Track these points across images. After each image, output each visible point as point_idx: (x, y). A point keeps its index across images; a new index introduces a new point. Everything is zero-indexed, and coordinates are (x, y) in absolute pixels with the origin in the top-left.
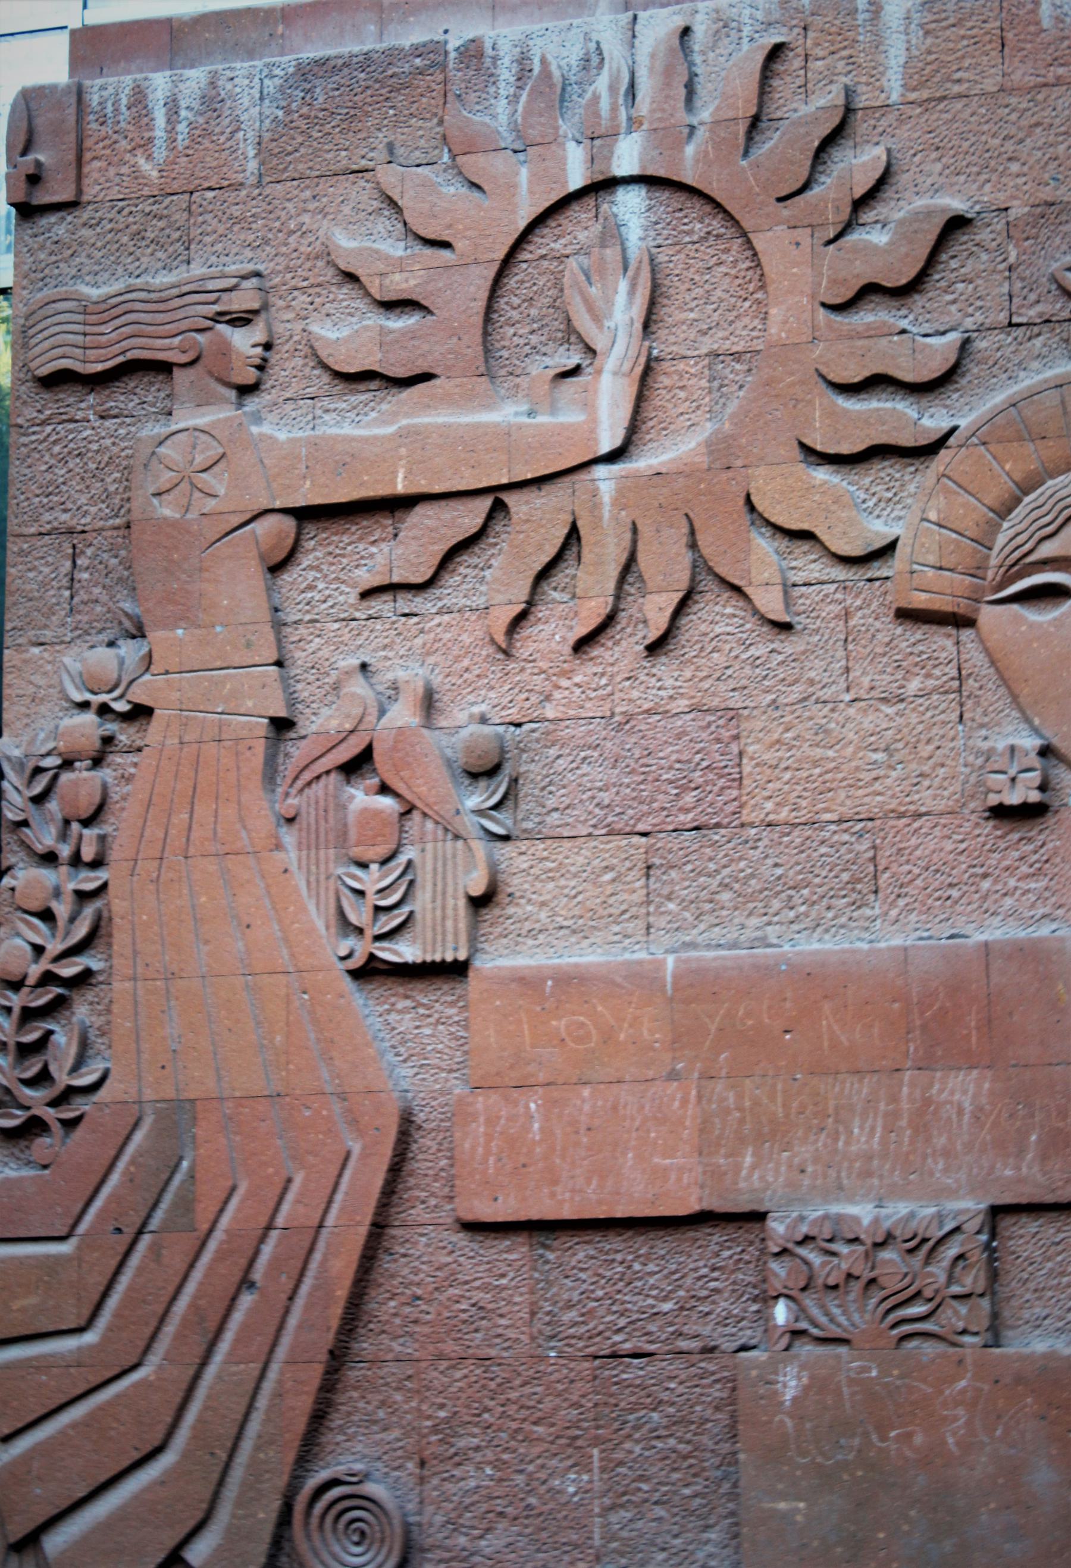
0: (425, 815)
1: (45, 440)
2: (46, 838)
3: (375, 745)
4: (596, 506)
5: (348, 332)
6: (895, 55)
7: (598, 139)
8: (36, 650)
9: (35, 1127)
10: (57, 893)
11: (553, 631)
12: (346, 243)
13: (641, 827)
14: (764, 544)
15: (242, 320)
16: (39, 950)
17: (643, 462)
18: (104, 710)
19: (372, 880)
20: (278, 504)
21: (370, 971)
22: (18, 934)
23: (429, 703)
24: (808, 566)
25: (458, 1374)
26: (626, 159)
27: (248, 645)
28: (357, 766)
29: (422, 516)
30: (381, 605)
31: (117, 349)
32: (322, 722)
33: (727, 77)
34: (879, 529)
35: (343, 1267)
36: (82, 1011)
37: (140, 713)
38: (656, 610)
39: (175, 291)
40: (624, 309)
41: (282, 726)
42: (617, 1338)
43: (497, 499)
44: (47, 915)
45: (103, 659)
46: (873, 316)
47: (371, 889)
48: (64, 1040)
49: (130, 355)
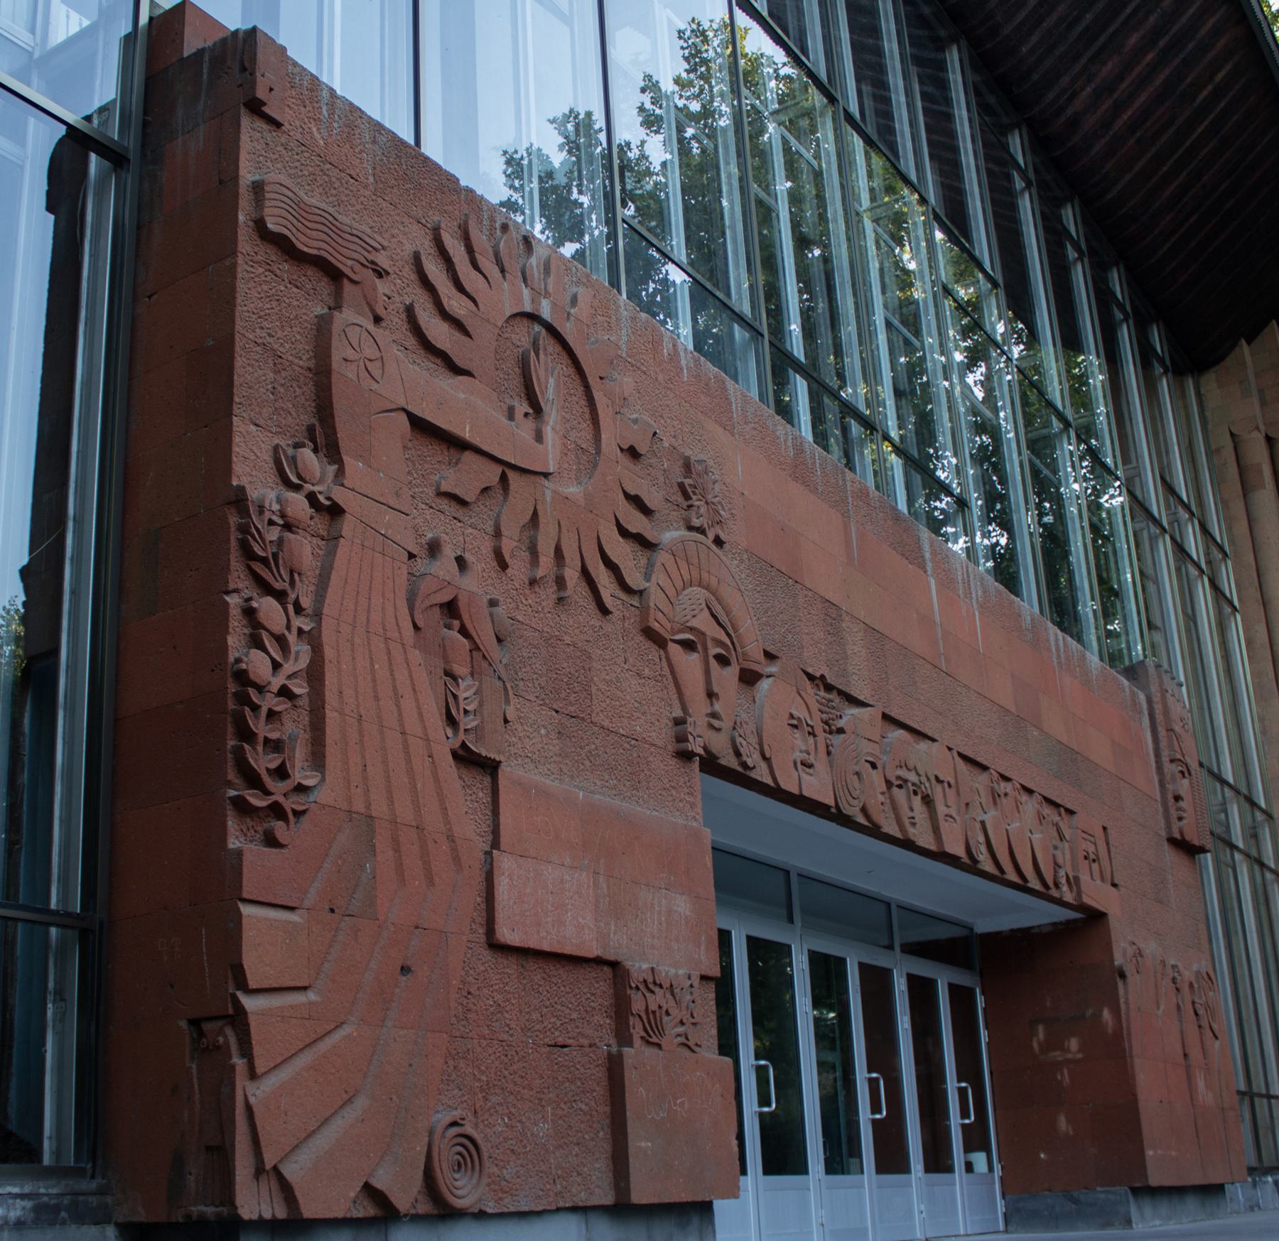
0: (484, 656)
1: (258, 276)
3: (460, 597)
4: (544, 501)
8: (253, 428)
10: (288, 628)
13: (555, 707)
15: (381, 274)
16: (276, 666)
18: (312, 498)
20: (410, 408)
22: (265, 650)
25: (490, 1050)
27: (397, 495)
30: (444, 504)
31: (316, 244)
37: (335, 511)
39: (348, 229)
42: (557, 1033)
44: (281, 640)
47: (462, 695)
49: (323, 253)
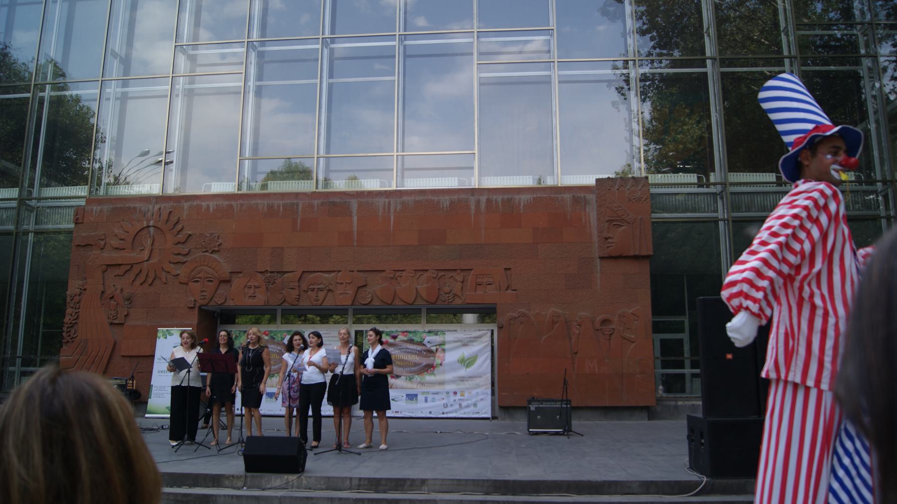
2: (72, 305)
5: (115, 242)
6: (185, 213)
7: (148, 221)
9: (68, 342)
11: (138, 282)
12: (116, 231)
14: (164, 274)
17: (150, 262)
19: (113, 312)
21: (111, 324)
23: (122, 290)
24: (169, 276)
26: (151, 223)
28: (112, 298)
29: (122, 267)
32: (108, 292)
33: (165, 216)
34: (178, 272)
35: (105, 360)
36: (75, 327)
37: (85, 289)
38: (150, 280)
40: (149, 242)
41: (103, 292)
43: (132, 265)
45: (81, 282)
46: (179, 246)
48: (73, 331)
